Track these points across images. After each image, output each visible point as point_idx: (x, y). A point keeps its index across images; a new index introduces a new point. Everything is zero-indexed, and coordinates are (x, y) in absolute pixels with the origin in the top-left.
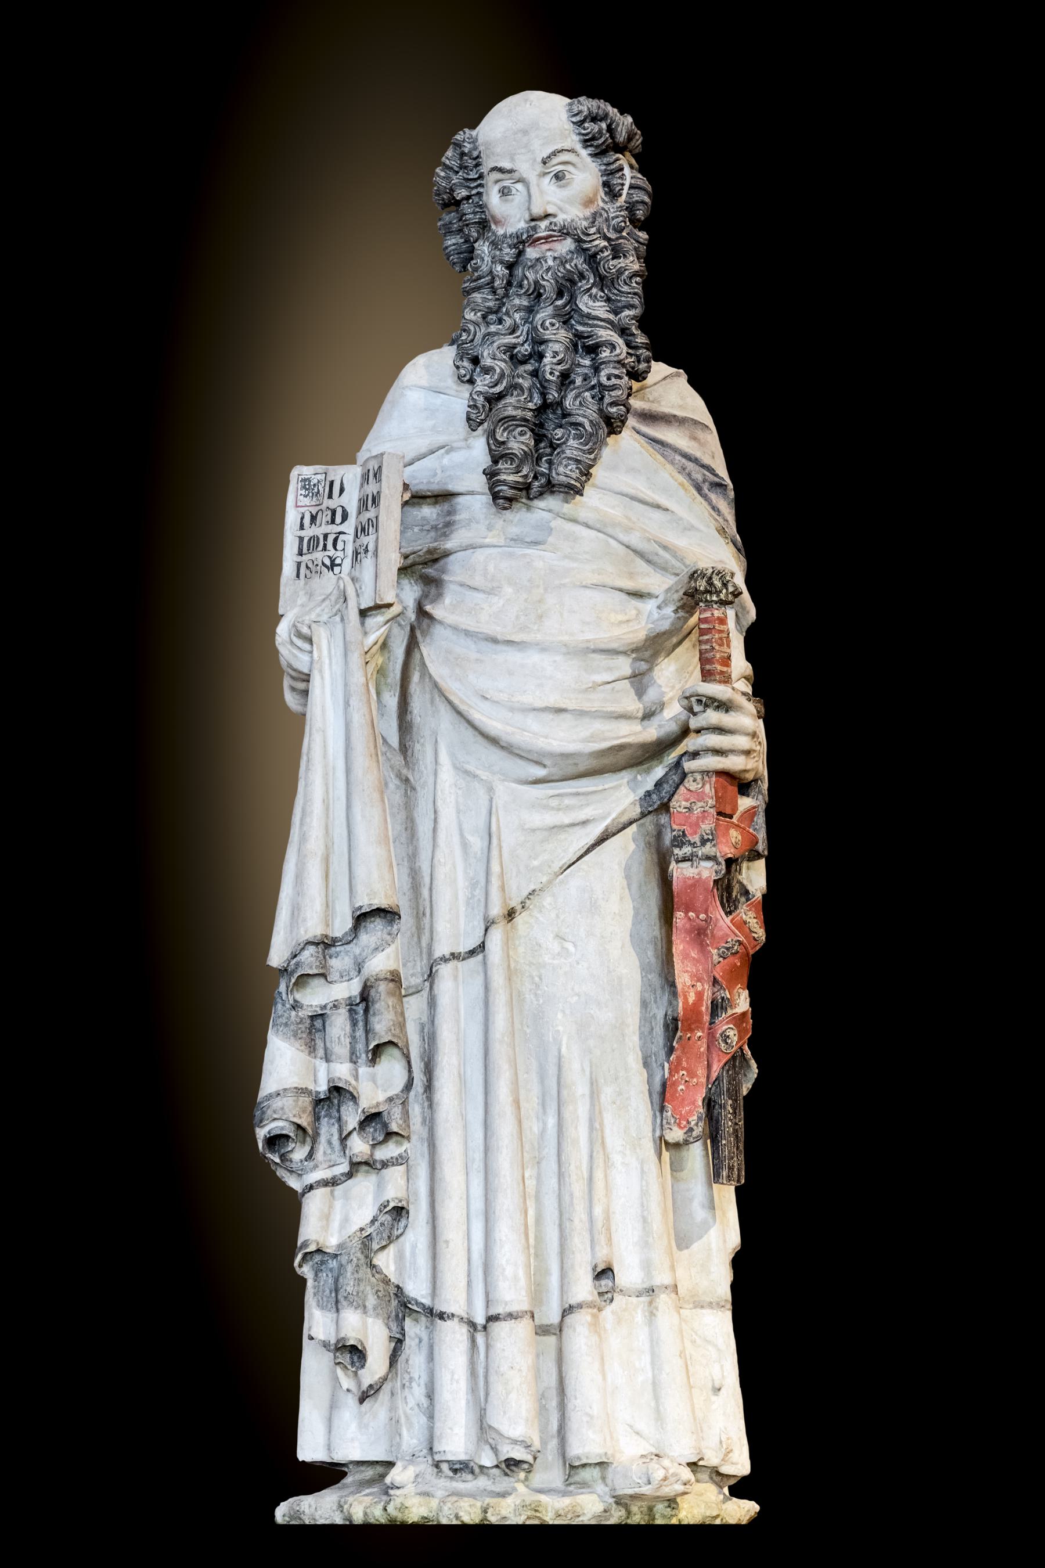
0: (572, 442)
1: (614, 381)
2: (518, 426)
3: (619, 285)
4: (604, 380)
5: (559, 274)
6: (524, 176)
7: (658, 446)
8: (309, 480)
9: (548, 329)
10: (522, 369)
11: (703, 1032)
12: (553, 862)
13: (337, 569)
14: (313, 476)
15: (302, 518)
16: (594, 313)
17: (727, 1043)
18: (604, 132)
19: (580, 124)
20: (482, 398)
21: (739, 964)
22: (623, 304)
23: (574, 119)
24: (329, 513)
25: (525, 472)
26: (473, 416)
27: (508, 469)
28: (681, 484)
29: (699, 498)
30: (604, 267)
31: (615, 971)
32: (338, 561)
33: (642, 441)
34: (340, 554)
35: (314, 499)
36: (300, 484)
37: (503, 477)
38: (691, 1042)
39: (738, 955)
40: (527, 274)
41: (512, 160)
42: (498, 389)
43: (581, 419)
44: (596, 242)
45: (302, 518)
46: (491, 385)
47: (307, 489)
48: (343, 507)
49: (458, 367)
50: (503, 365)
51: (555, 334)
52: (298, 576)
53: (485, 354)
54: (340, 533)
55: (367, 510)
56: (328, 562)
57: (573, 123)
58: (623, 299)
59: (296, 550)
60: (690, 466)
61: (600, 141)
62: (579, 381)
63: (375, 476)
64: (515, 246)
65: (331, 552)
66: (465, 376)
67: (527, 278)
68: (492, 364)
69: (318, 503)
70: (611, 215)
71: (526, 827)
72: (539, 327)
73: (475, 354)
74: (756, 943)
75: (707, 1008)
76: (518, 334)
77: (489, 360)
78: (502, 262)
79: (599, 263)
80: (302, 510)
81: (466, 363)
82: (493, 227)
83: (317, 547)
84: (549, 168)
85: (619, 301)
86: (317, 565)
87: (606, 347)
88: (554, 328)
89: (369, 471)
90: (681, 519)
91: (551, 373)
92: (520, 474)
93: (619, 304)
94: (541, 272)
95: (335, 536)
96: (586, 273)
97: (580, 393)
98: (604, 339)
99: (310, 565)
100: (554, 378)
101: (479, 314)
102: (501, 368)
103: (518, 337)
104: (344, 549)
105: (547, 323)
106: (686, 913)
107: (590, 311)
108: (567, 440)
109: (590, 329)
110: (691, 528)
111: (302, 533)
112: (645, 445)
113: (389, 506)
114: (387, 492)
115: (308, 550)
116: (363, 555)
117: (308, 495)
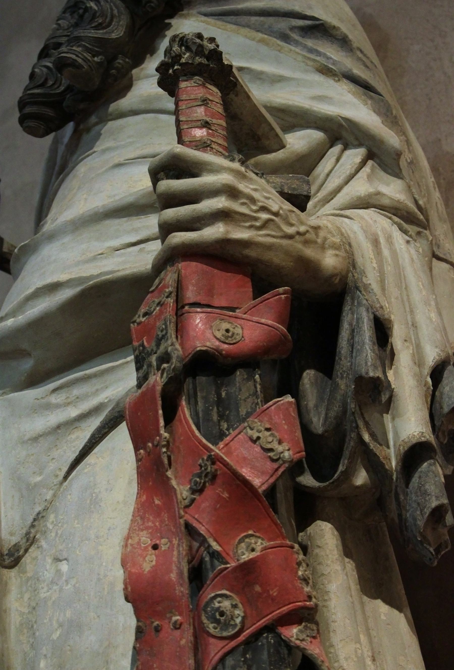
7: (233, 18)
11: (180, 615)
12: (60, 469)
17: (218, 622)
21: (226, 495)
28: (261, 41)
31: (106, 576)
38: (162, 634)
39: (219, 481)
60: (270, 20)
71: (26, 438)
74: (275, 465)
75: (180, 574)
106: (145, 449)
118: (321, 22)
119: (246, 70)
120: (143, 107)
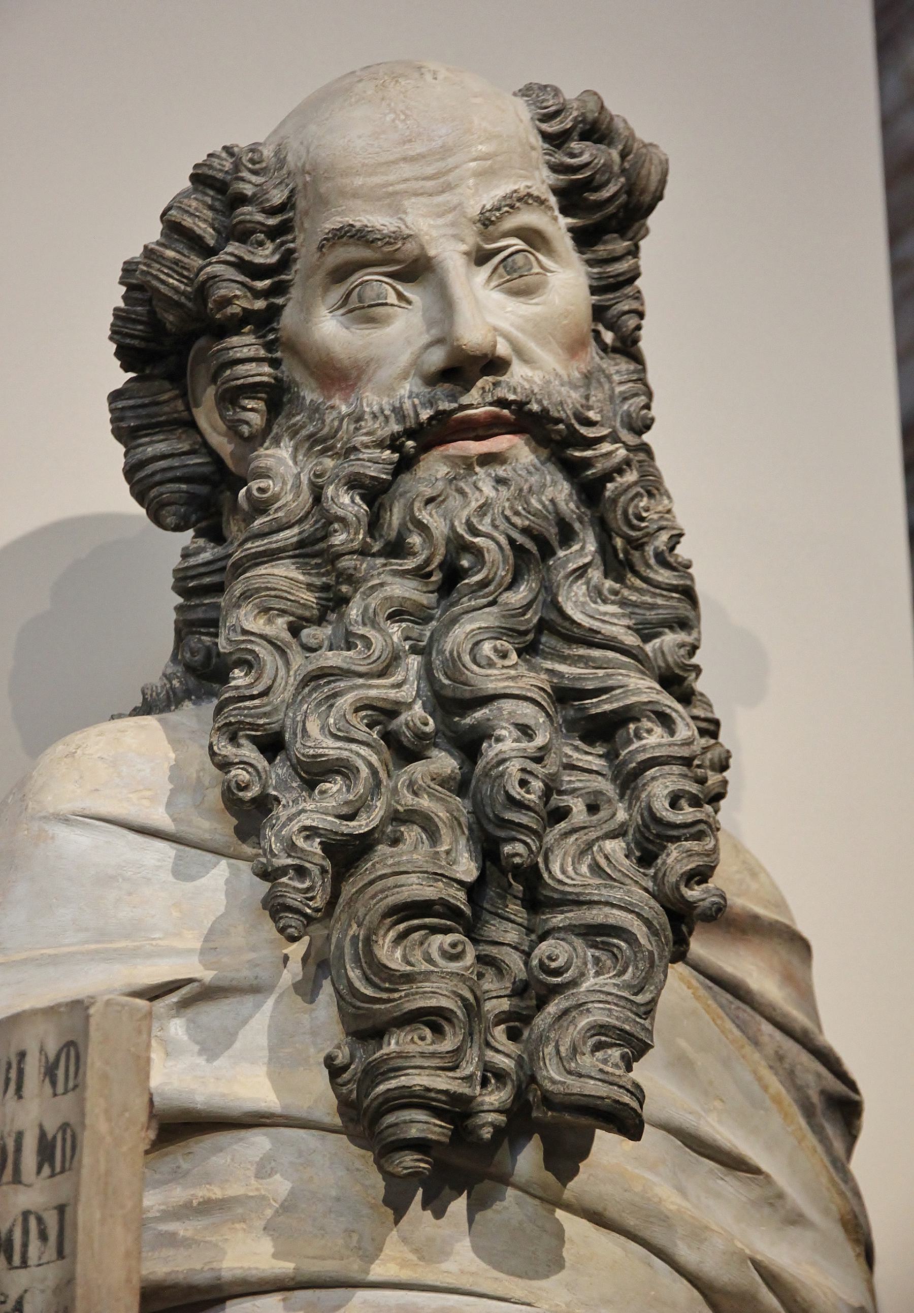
0: (589, 983)
1: (688, 814)
2: (435, 930)
3: (648, 566)
4: (662, 807)
5: (517, 520)
6: (432, 253)
9: (491, 664)
10: (418, 769)
16: (607, 629)
18: (616, 168)
19: (556, 140)
20: (315, 846)
22: (663, 614)
23: (545, 127)
25: (468, 1069)
26: (294, 899)
27: (433, 1055)
29: (812, 1139)
30: (625, 513)
33: (695, 983)
37: (418, 1080)
40: (425, 516)
41: (397, 210)
42: (361, 825)
43: (617, 917)
44: (606, 447)
46: (345, 810)
49: (224, 765)
50: (374, 759)
51: (513, 678)
53: (313, 727)
57: (546, 136)
58: (660, 601)
61: (606, 193)
62: (578, 806)
63: (50, 1072)
64: (394, 444)
67: (423, 528)
68: (345, 754)
70: (619, 389)
72: (467, 659)
76: (398, 677)
77: (331, 742)
78: (354, 483)
79: (614, 501)
81: (249, 752)
82: (310, 395)
84: (495, 241)
85: (653, 607)
87: (649, 719)
88: (507, 663)
89: (22, 1055)
90: (781, 1196)
91: (523, 783)
92: (458, 1074)
93: (651, 615)
94: (464, 514)
96: (577, 526)
97: (590, 845)
98: (644, 698)
100: (532, 797)
101: (281, 622)
102: (370, 765)
103: (399, 685)
105: (487, 648)
107: (596, 625)
108: (582, 974)
109: (601, 672)
110: (796, 1219)
112: (702, 992)
113: (108, 1173)
114: (103, 1127)
118: (856, 1097)
119: (761, 1177)
120: (631, 1222)
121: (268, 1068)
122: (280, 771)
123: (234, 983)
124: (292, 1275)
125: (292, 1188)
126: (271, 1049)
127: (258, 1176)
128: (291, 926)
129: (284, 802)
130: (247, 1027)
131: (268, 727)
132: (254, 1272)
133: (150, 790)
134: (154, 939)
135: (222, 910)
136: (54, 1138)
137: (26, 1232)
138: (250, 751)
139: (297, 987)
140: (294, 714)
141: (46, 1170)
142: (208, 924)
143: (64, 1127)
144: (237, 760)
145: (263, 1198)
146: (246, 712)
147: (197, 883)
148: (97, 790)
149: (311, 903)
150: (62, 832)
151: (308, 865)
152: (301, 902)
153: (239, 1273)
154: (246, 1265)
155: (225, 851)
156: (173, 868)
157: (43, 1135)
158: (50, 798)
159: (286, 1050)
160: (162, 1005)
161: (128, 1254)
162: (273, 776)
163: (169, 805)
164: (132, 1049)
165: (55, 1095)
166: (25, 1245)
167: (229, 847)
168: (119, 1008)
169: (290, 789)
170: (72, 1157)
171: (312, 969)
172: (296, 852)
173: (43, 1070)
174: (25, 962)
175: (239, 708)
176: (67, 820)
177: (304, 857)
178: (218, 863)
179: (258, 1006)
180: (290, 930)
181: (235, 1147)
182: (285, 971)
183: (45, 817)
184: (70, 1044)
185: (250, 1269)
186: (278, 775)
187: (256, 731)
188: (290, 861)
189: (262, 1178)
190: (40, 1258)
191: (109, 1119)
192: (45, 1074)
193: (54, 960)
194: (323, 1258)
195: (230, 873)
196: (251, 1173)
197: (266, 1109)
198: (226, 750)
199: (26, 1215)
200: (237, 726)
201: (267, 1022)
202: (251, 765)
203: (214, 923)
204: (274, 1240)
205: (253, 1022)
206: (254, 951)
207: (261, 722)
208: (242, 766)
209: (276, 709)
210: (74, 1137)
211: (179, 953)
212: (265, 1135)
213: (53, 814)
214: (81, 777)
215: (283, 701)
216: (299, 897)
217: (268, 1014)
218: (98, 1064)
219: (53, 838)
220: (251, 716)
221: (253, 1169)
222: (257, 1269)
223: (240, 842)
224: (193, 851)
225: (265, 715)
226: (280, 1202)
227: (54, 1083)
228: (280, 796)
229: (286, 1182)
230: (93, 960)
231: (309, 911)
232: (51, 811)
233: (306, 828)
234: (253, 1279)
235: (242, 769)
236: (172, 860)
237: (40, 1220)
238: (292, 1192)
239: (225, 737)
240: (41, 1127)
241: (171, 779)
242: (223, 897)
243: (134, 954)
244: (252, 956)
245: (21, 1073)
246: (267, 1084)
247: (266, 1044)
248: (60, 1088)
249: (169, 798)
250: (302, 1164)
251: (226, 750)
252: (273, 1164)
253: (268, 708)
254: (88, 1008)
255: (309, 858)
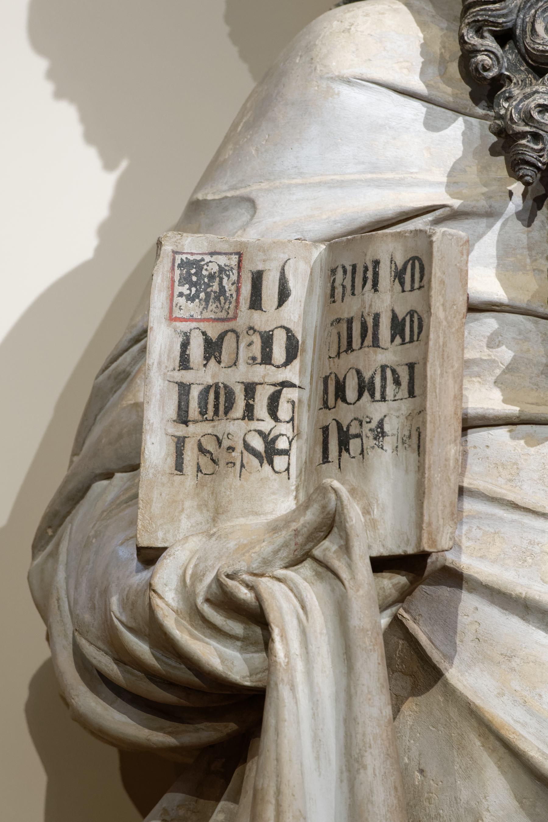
8: (198, 265)
13: (280, 462)
14: (207, 258)
15: (185, 345)
24: (257, 340)
32: (282, 444)
34: (285, 429)
35: (212, 306)
36: (177, 272)
45: (185, 345)
47: (192, 284)
48: (288, 330)
52: (179, 467)
54: (285, 384)
55: (376, 343)
56: (258, 444)
59: (172, 411)
63: (399, 275)
65: (267, 425)
66: (485, 69)
69: (223, 315)
73: (510, 25)
80: (185, 326)
83: (228, 409)
86: (231, 449)
89: (376, 263)
95: (272, 390)
99: (210, 446)
104: (292, 419)
111: (187, 377)
113: (445, 344)
114: (441, 314)
115: (203, 413)
116: (370, 442)
117: (197, 296)
121: (497, 271)
122: (510, 57)
123: (475, 209)
124: (518, 415)
125: (515, 356)
126: (499, 258)
127: (489, 347)
128: (528, 175)
129: (515, 80)
130: (482, 241)
131: (505, 24)
132: (491, 411)
133: (407, 62)
134: (412, 173)
135: (460, 154)
136: (404, 319)
137: (384, 379)
138: (492, 42)
139: (519, 215)
140: (524, 16)
141: (398, 340)
142: (450, 164)
143: (412, 313)
144: (483, 49)
145: (494, 361)
146: (490, 13)
147: (442, 133)
148: (370, 60)
149: (541, 159)
150: (344, 90)
151: (541, 132)
152: (536, 159)
153: (480, 411)
154: (486, 406)
155: (463, 111)
156: (424, 120)
157: (394, 317)
158: (334, 64)
159: (510, 259)
160: (420, 221)
161: (455, 397)
162: (505, 60)
163: (423, 74)
164: (458, 265)
165: (403, 291)
166: (384, 387)
167: (466, 108)
168: (450, 237)
169: (519, 71)
170: (419, 333)
171: (530, 202)
172: (533, 123)
173: (393, 274)
174: (320, 184)
175: (485, 10)
176: (349, 82)
177: (540, 127)
178: (455, 120)
179: (490, 227)
180: (528, 178)
181: (471, 324)
182: (511, 203)
183: (332, 78)
184: (414, 259)
185: (488, 409)
186: (508, 59)
187: (496, 27)
188: (527, 129)
189: (492, 348)
190: (395, 396)
191: (445, 310)
192: (395, 277)
193: (341, 184)
194: (537, 404)
195: (465, 127)
196: (484, 343)
197: (498, 300)
198: (472, 39)
199: (383, 368)
200: (483, 22)
201: (496, 238)
202: (493, 53)
203: (455, 163)
204: (502, 390)
205: (486, 238)
206: (485, 186)
207: (500, 21)
208: (486, 53)
209: (511, 12)
210: (420, 320)
211: (432, 184)
212: (493, 317)
213: (338, 76)
214: (357, 50)
215: (516, 6)
216: (535, 155)
217: (497, 233)
218: (439, 274)
219: (338, 94)
220: (494, 16)
221: (485, 340)
222: (494, 409)
223: (474, 105)
224: (439, 108)
225: (503, 16)
226: (506, 365)
227: (402, 284)
228: (512, 76)
229: (510, 351)
230: (369, 186)
231: (540, 165)
232: (337, 74)
233: (539, 105)
234: (491, 416)
235: (486, 55)
236: (423, 115)
237: (394, 371)
238: (514, 359)
239: (472, 30)
240: (393, 311)
241: (422, 54)
242: (461, 145)
243: (400, 183)
244: (485, 190)
245: (376, 275)
246: (498, 283)
247: (495, 254)
248: (408, 286)
249: (422, 68)
250: (521, 340)
251: (472, 39)
252: (500, 338)
253: (505, 11)
254: (430, 236)
255: (543, 128)
